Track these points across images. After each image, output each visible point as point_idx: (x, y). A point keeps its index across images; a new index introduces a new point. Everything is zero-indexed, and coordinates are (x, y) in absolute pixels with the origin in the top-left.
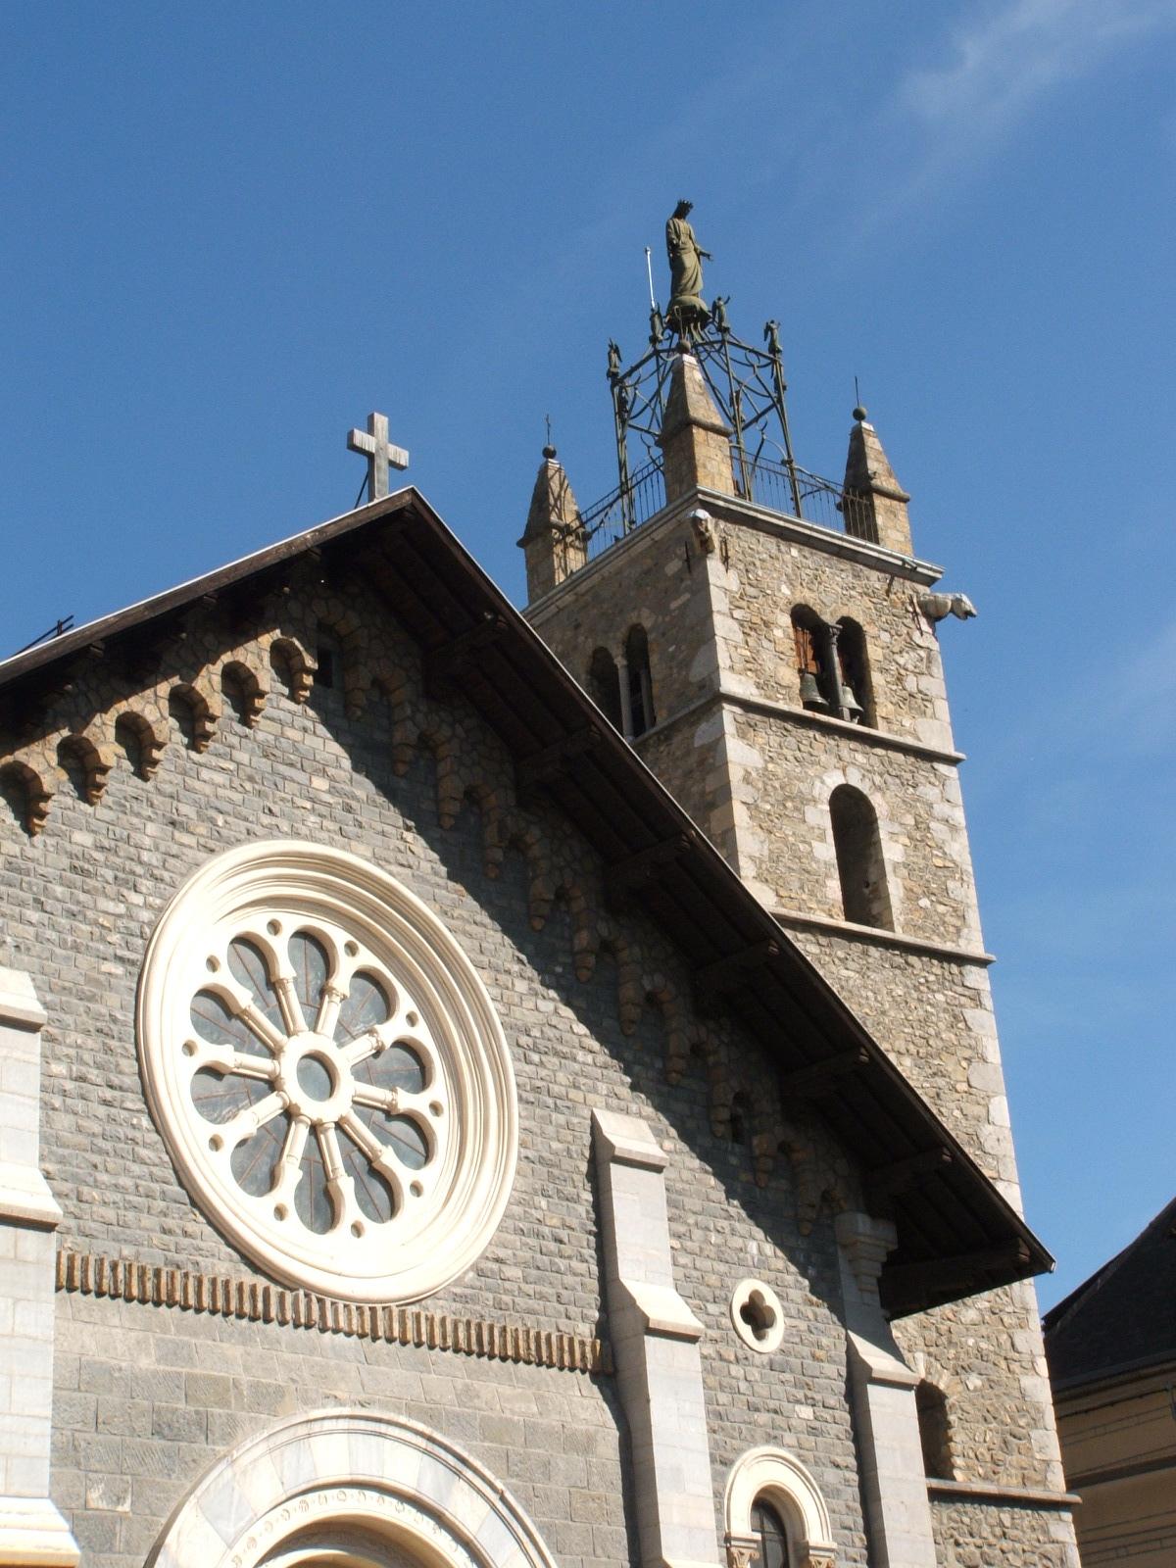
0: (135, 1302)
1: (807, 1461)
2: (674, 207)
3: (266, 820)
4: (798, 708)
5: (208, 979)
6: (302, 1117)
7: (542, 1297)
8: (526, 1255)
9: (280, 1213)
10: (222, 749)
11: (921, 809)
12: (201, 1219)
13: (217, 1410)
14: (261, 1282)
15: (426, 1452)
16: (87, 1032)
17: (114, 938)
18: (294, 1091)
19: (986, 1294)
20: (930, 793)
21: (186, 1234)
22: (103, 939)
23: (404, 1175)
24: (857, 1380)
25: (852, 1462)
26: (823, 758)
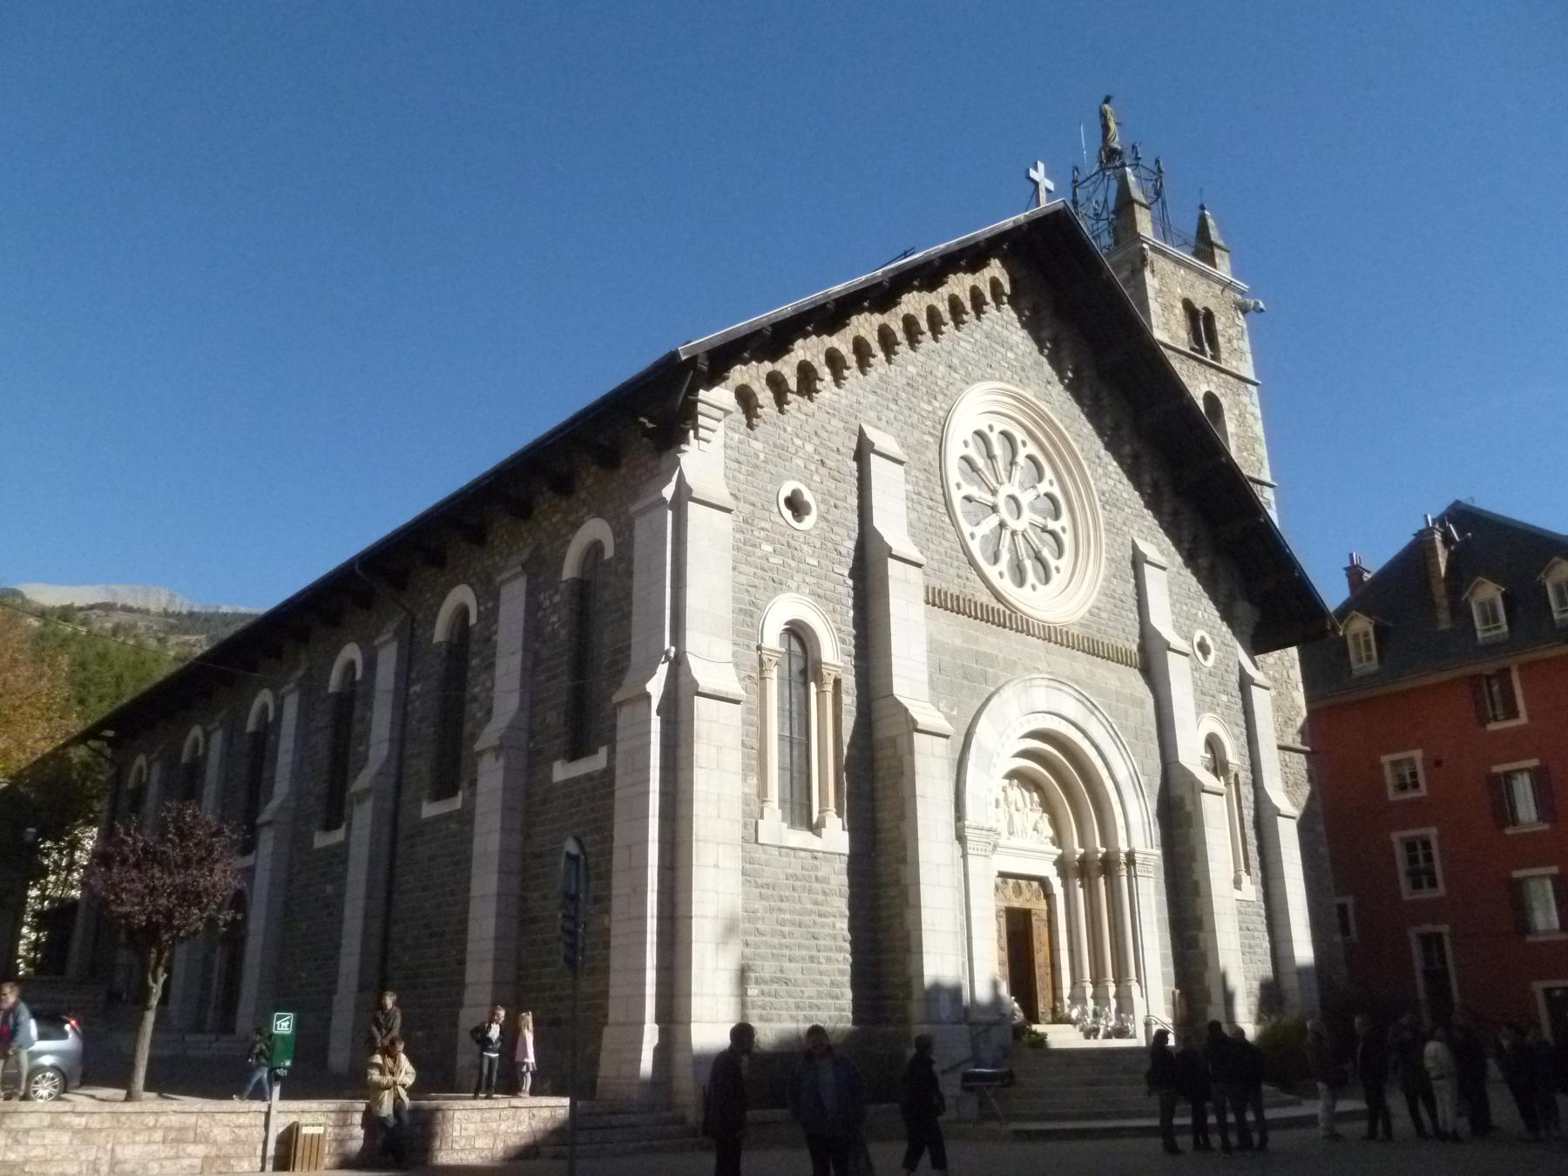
1: (1225, 720)
2: (1103, 99)
3: (989, 370)
4: (1188, 350)
5: (965, 452)
7: (1116, 628)
8: (1109, 607)
9: (1001, 574)
10: (969, 332)
11: (1241, 406)
12: (974, 572)
13: (991, 670)
14: (1002, 608)
15: (1078, 700)
16: (919, 470)
17: (928, 423)
18: (1004, 514)
19: (1278, 651)
20: (1245, 399)
21: (967, 579)
22: (923, 423)
23: (1052, 562)
24: (1245, 683)
25: (1244, 725)
26: (1200, 377)
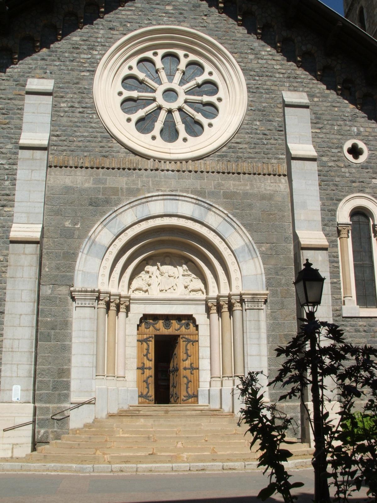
0: (89, 168)
6: (164, 109)
15: (196, 204)
17: (86, 65)
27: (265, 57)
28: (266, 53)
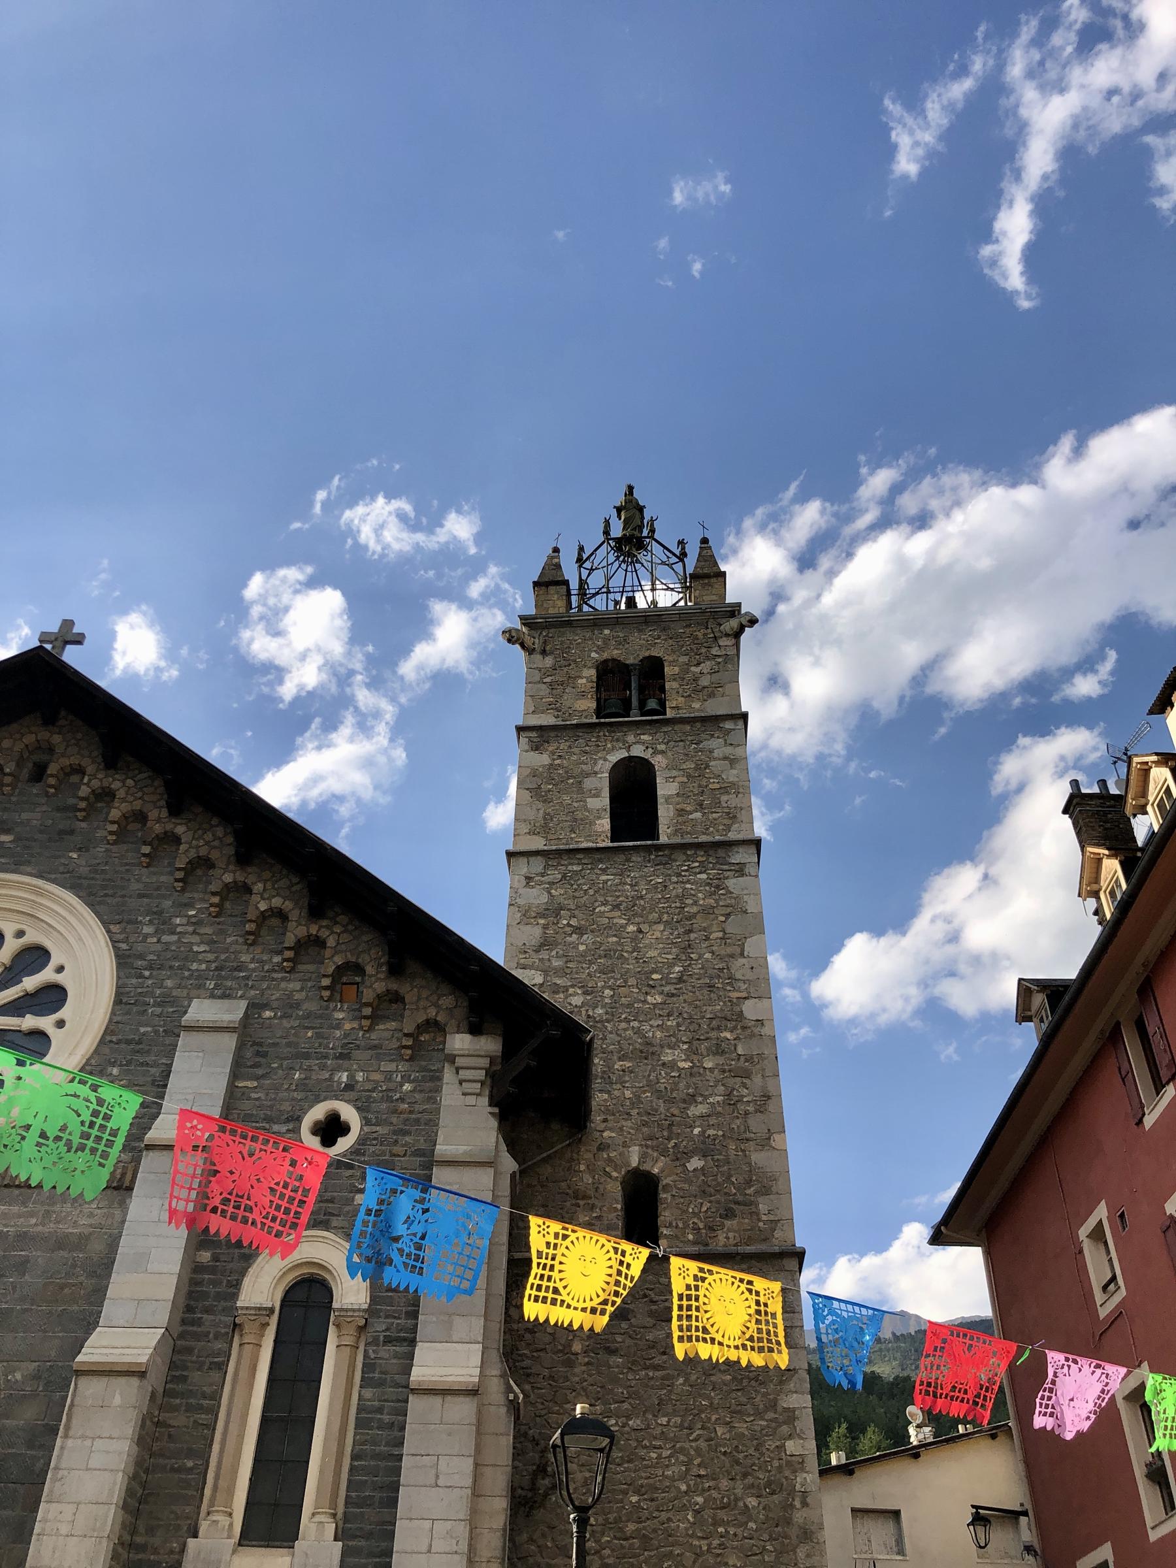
27: (178, 930)
28: (184, 921)
